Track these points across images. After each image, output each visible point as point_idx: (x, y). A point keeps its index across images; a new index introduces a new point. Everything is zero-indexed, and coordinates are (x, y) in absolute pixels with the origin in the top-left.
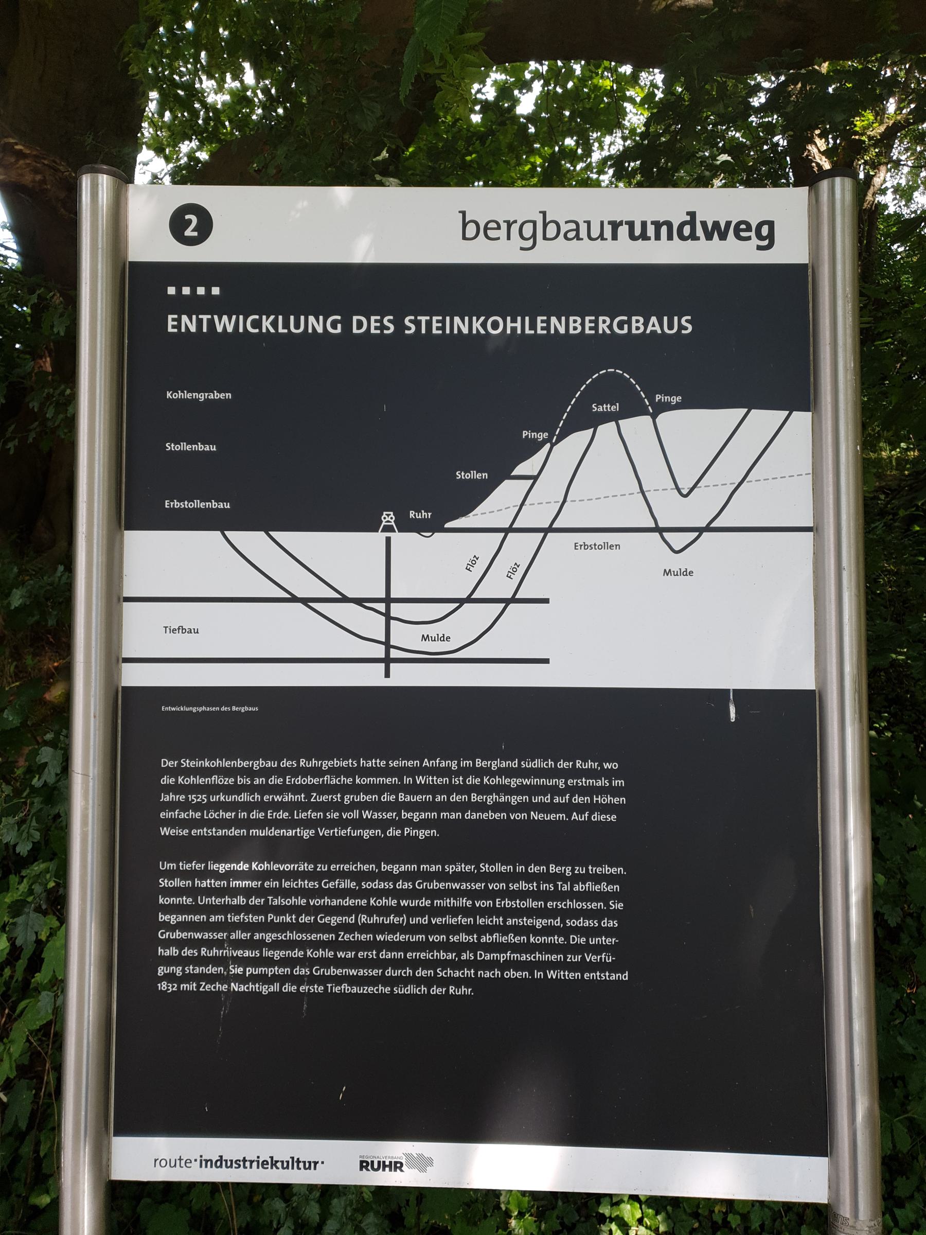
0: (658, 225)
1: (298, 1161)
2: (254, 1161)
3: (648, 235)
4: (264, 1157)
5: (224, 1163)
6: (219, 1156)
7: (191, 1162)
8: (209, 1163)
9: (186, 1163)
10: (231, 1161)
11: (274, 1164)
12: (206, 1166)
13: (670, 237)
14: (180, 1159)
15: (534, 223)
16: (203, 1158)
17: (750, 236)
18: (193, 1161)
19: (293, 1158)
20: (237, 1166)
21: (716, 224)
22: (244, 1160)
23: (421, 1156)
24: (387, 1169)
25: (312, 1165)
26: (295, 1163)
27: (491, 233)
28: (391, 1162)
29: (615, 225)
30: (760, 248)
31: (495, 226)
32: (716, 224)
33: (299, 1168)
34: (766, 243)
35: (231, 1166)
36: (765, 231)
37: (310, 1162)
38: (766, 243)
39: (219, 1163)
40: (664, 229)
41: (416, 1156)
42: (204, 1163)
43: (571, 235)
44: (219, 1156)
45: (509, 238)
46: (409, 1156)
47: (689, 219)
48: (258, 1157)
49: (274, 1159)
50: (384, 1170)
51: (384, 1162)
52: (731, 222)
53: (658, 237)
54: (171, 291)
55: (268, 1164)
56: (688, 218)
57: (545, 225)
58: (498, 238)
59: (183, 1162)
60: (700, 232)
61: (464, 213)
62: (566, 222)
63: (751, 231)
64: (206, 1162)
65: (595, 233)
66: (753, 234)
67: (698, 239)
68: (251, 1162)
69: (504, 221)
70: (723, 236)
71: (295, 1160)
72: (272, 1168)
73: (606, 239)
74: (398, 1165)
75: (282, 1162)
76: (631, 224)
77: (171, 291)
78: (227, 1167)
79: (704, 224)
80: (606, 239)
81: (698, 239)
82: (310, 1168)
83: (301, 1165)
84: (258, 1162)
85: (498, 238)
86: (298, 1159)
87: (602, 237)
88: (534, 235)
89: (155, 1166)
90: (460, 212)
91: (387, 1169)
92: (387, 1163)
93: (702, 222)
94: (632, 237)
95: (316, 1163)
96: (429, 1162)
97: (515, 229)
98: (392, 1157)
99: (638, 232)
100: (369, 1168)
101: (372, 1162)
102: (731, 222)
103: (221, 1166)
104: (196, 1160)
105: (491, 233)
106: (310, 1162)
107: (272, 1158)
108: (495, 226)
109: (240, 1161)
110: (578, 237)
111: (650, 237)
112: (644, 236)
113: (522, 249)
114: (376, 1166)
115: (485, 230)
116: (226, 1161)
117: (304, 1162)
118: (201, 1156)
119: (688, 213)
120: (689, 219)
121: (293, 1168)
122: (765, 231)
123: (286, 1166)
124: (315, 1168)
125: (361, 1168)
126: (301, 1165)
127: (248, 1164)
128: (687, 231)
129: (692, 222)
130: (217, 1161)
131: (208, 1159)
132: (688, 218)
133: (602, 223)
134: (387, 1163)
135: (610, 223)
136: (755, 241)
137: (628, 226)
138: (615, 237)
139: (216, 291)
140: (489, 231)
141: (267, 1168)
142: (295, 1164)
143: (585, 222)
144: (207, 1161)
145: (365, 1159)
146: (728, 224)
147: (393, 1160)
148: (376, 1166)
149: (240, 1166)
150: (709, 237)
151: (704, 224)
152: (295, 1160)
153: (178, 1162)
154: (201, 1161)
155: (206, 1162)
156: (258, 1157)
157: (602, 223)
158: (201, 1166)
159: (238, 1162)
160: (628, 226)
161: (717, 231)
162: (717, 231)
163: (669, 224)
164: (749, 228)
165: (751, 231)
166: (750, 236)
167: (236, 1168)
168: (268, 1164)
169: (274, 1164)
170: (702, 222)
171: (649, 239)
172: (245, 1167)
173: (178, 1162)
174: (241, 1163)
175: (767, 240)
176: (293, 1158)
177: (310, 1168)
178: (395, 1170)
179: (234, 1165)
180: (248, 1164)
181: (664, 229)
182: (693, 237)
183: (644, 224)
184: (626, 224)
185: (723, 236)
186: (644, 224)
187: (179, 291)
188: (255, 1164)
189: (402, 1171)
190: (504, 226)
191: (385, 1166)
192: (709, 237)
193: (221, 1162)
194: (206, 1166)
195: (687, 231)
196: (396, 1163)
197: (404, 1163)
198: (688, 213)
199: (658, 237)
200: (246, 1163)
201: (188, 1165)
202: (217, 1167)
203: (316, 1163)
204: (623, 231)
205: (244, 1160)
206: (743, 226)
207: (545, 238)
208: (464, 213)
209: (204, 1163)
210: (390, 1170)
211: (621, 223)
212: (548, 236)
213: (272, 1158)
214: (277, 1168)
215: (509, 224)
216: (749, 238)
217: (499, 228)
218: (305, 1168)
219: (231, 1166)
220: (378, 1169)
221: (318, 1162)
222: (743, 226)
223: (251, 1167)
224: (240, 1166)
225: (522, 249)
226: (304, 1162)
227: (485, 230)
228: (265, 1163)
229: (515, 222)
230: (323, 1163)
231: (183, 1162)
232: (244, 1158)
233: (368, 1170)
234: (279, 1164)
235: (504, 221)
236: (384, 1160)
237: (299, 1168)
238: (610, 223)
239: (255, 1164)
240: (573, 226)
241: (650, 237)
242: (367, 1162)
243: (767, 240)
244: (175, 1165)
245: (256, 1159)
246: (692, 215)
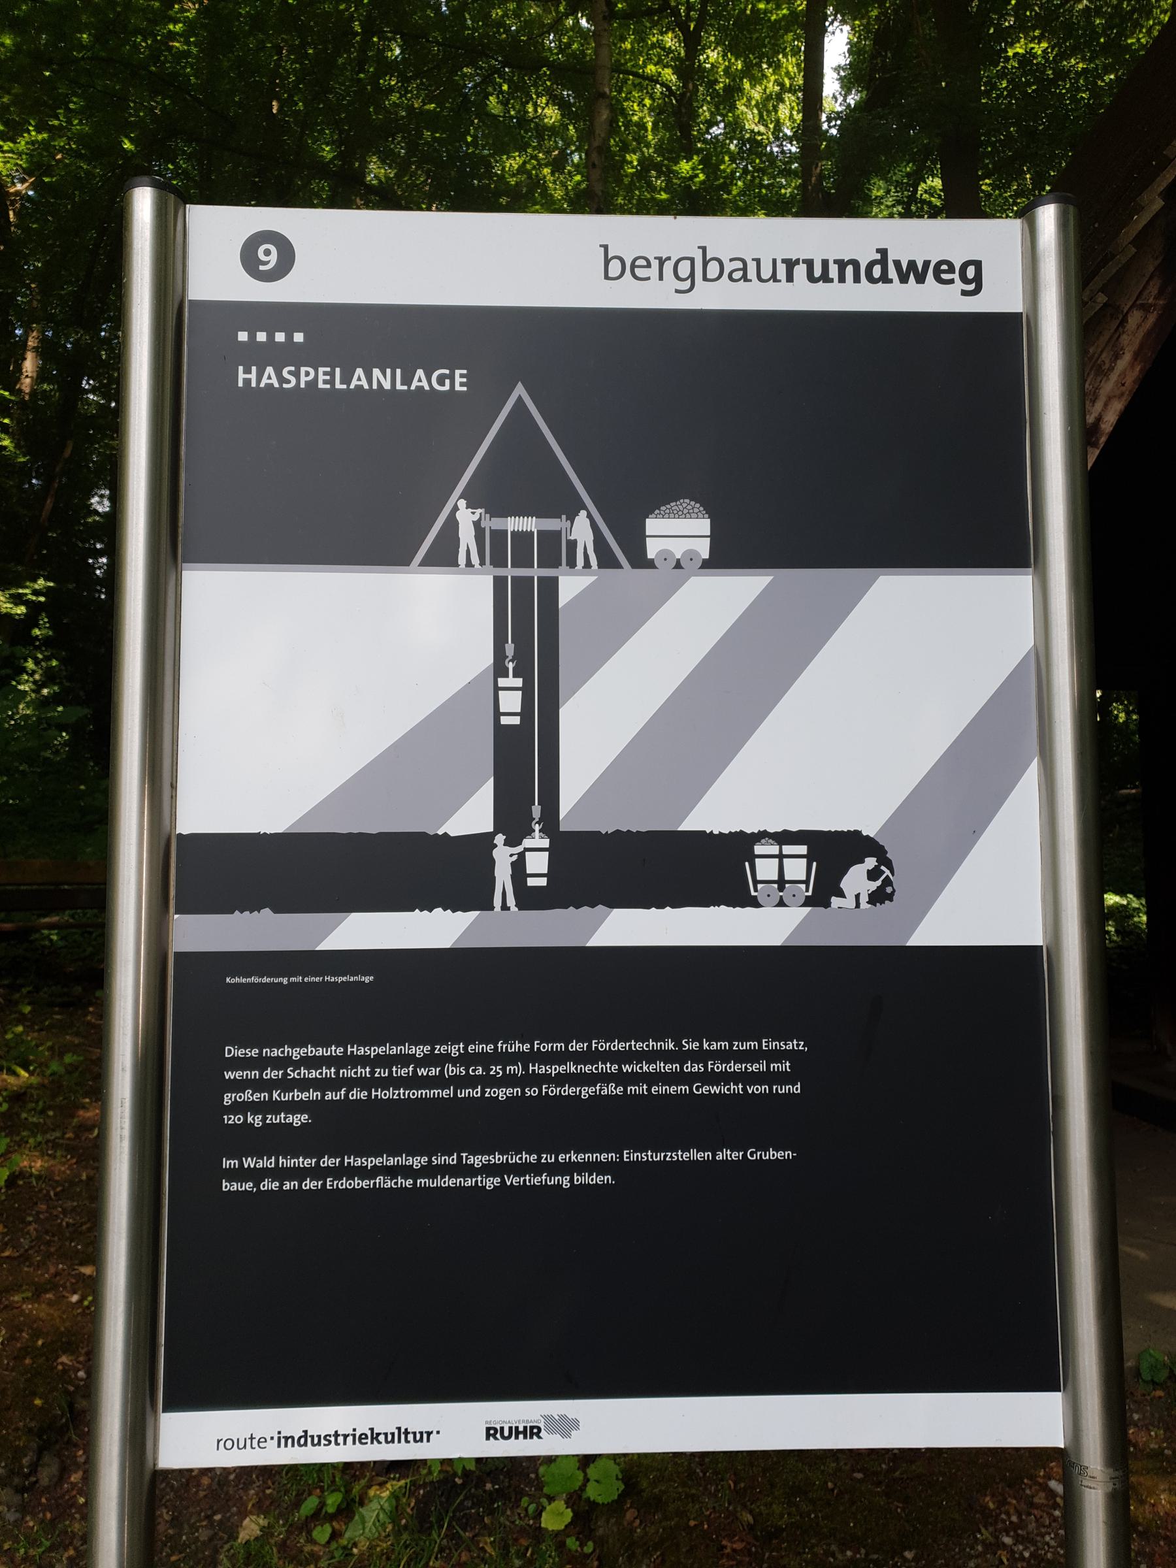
0: (842, 265)
1: (407, 1433)
2: (348, 1435)
3: (831, 276)
5: (309, 1440)
6: (303, 1431)
7: (266, 1441)
8: (290, 1441)
9: (259, 1442)
10: (319, 1437)
11: (375, 1437)
12: (286, 1445)
13: (857, 279)
14: (252, 1438)
15: (692, 260)
16: (282, 1435)
17: (953, 279)
18: (268, 1439)
19: (399, 1429)
20: (327, 1443)
21: (912, 264)
22: (336, 1435)
24: (521, 1436)
25: (425, 1436)
26: (403, 1434)
27: (639, 272)
28: (525, 1428)
29: (790, 264)
30: (965, 293)
31: (644, 263)
32: (912, 264)
33: (407, 1441)
34: (972, 287)
35: (319, 1443)
36: (971, 272)
37: (421, 1433)
38: (972, 287)
40: (849, 270)
41: (557, 1418)
42: (283, 1441)
43: (737, 275)
44: (303, 1431)
45: (661, 278)
46: (548, 1418)
47: (879, 258)
48: (354, 1430)
49: (375, 1431)
50: (517, 1438)
51: (517, 1428)
52: (930, 261)
53: (842, 279)
55: (367, 1437)
56: (878, 256)
57: (705, 264)
58: (648, 279)
59: (255, 1442)
60: (892, 273)
61: (606, 247)
62: (731, 260)
63: (954, 273)
64: (285, 1440)
65: (766, 273)
66: (956, 276)
67: (891, 281)
68: (346, 1436)
69: (655, 258)
70: (921, 279)
71: (403, 1430)
72: (372, 1443)
73: (780, 281)
74: (535, 1431)
75: (386, 1434)
76: (810, 263)
77: (243, 336)
78: (313, 1445)
79: (897, 264)
80: (780, 281)
81: (891, 281)
82: (421, 1440)
83: (410, 1437)
84: (354, 1436)
85: (648, 279)
86: (406, 1430)
87: (774, 278)
88: (692, 275)
89: (218, 1449)
90: (601, 246)
91: (521, 1436)
92: (521, 1429)
93: (894, 261)
94: (811, 278)
95: (429, 1434)
97: (668, 267)
98: (527, 1421)
99: (818, 272)
100: (498, 1436)
101: (502, 1429)
102: (929, 262)
103: (305, 1444)
104: (272, 1438)
105: (639, 272)
106: (421, 1433)
107: (372, 1430)
108: (644, 263)
109: (330, 1436)
110: (745, 278)
111: (833, 279)
112: (825, 278)
113: (677, 291)
114: (506, 1434)
115: (632, 268)
116: (312, 1437)
117: (414, 1433)
118: (279, 1433)
119: (878, 251)
120: (879, 258)
121: (399, 1441)
122: (971, 272)
123: (390, 1439)
124: (428, 1440)
125: (488, 1438)
126: (410, 1437)
127: (340, 1440)
128: (877, 271)
129: (883, 262)
130: (300, 1438)
131: (289, 1435)
132: (878, 256)
133: (774, 261)
134: (521, 1429)
135: (784, 261)
136: (959, 285)
137: (805, 265)
138: (790, 278)
139: (299, 337)
140: (636, 269)
141: (366, 1443)
142: (403, 1436)
143: (753, 260)
144: (286, 1438)
145: (493, 1426)
146: (927, 264)
147: (528, 1425)
148: (506, 1434)
149: (330, 1442)
150: (904, 279)
151: (897, 264)
152: (403, 1430)
153: (248, 1442)
154: (279, 1439)
155: (285, 1440)
156: (354, 1430)
157: (774, 261)
158: (279, 1446)
159: (328, 1438)
160: (805, 265)
161: (913, 272)
162: (913, 272)
163: (855, 264)
164: (951, 269)
165: (954, 273)
166: (953, 279)
167: (325, 1445)
168: (367, 1437)
169: (375, 1437)
170: (894, 261)
171: (831, 281)
172: (337, 1444)
173: (248, 1442)
174: (333, 1439)
175: (974, 285)
176: (399, 1429)
177: (421, 1440)
178: (531, 1437)
179: (323, 1442)
180: (340, 1440)
181: (849, 270)
182: (885, 278)
183: (825, 263)
184: (803, 263)
185: (921, 279)
186: (825, 263)
187: (252, 336)
188: (350, 1439)
189: (540, 1437)
190: (655, 264)
191: (518, 1433)
192: (904, 279)
193: (305, 1439)
194: (286, 1445)
195: (877, 271)
196: (532, 1428)
197: (542, 1428)
198: (878, 251)
199: (842, 279)
200: (339, 1438)
201: (261, 1445)
202: (300, 1445)
203: (429, 1434)
204: (800, 271)
205: (336, 1435)
206: (944, 267)
207: (705, 278)
208: (606, 247)
209: (283, 1441)
210: (525, 1437)
211: (797, 262)
212: (709, 277)
213: (372, 1430)
214: (379, 1442)
215: (662, 262)
216: (952, 281)
217: (649, 265)
218: (415, 1441)
219: (319, 1443)
221: (432, 1432)
222: (944, 267)
223: (345, 1443)
224: (330, 1442)
225: (677, 291)
226: (414, 1433)
227: (632, 268)
228: (363, 1436)
229: (669, 258)
230: (438, 1432)
231: (255, 1442)
232: (336, 1432)
233: (496, 1439)
234: (382, 1438)
235: (655, 258)
236: (517, 1425)
237: (407, 1441)
238: (784, 261)
239: (350, 1439)
240: (740, 265)
241: (833, 279)
242: (495, 1429)
243: (974, 284)
244: (245, 1447)
245: (352, 1432)
246: (883, 252)
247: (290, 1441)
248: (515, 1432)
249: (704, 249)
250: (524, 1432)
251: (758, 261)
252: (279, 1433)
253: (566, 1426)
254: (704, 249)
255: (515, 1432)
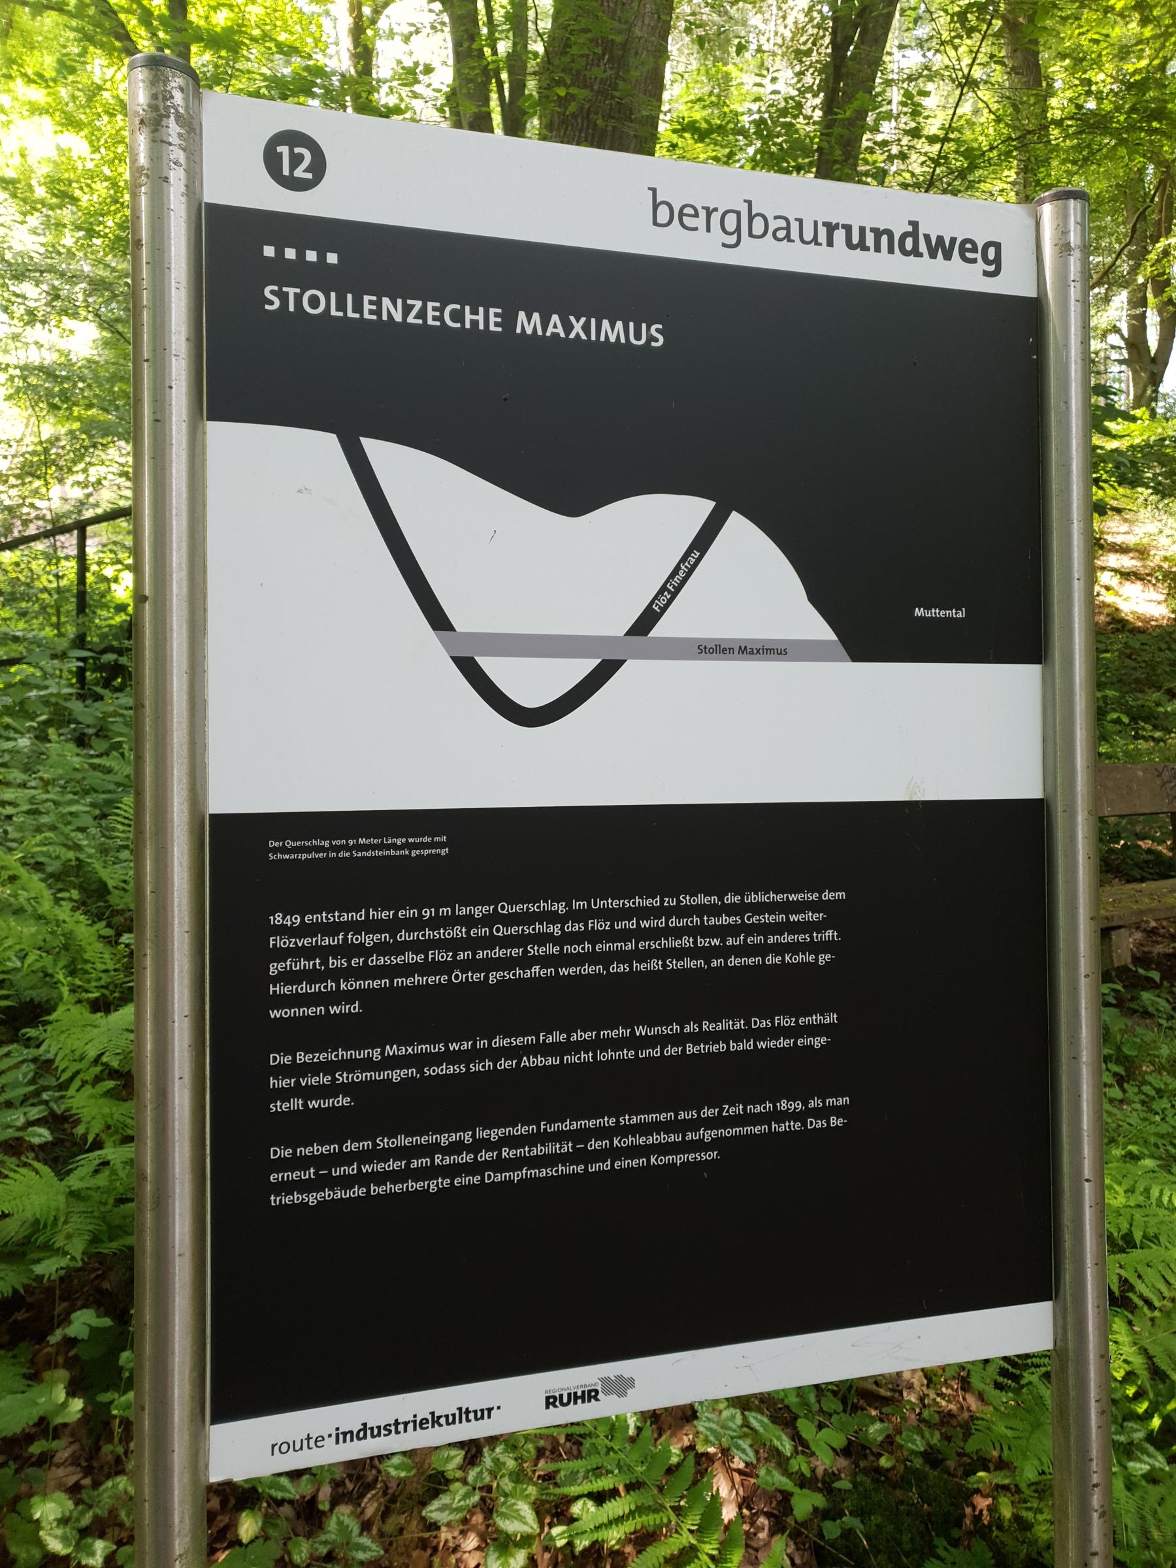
0: (878, 234)
1: (468, 1412)
4: (424, 1414)
5: (369, 1432)
9: (316, 1441)
12: (345, 1441)
14: (309, 1438)
15: (738, 214)
18: (326, 1437)
21: (940, 239)
23: (620, 1378)
24: (579, 1401)
25: (486, 1413)
27: (688, 221)
28: (583, 1392)
29: (831, 228)
30: (986, 274)
32: (940, 239)
33: (468, 1420)
34: (992, 268)
35: (379, 1434)
37: (482, 1411)
38: (992, 268)
39: (362, 1434)
40: (884, 239)
42: (341, 1437)
45: (708, 230)
50: (575, 1403)
51: (575, 1393)
54: (269, 251)
55: (427, 1422)
56: (910, 229)
59: (312, 1442)
60: (923, 248)
62: (776, 218)
64: (343, 1436)
65: (808, 236)
66: (978, 256)
68: (406, 1424)
69: (703, 208)
70: (948, 256)
75: (447, 1416)
76: (848, 229)
81: (921, 255)
83: (471, 1416)
84: (415, 1422)
91: (579, 1401)
92: (579, 1394)
94: (850, 245)
95: (490, 1410)
96: (630, 1383)
97: (715, 218)
99: (855, 240)
100: (557, 1403)
101: (561, 1396)
104: (330, 1436)
105: (688, 221)
110: (788, 237)
112: (862, 245)
113: (724, 245)
114: (565, 1400)
116: (372, 1429)
117: (475, 1412)
119: (911, 223)
123: (451, 1420)
124: (489, 1417)
125: (547, 1407)
126: (471, 1416)
127: (401, 1428)
129: (914, 234)
132: (910, 229)
133: (816, 223)
134: (579, 1394)
136: (981, 266)
138: (830, 243)
140: (684, 218)
142: (464, 1416)
144: (345, 1434)
146: (953, 240)
148: (565, 1400)
149: (390, 1431)
150: (933, 255)
153: (305, 1442)
154: (337, 1435)
156: (415, 1416)
157: (816, 223)
158: (337, 1442)
168: (427, 1422)
169: (436, 1420)
171: (868, 249)
172: (397, 1432)
173: (305, 1442)
174: (393, 1428)
176: (460, 1409)
177: (482, 1417)
178: (589, 1401)
179: (383, 1432)
180: (401, 1428)
182: (916, 252)
185: (948, 256)
188: (410, 1426)
189: (597, 1400)
191: (576, 1398)
194: (345, 1441)
196: (590, 1391)
198: (911, 223)
203: (490, 1410)
204: (840, 235)
205: (397, 1423)
206: (968, 246)
207: (751, 235)
209: (341, 1437)
210: (583, 1402)
211: (837, 226)
213: (433, 1414)
214: (440, 1425)
215: (709, 212)
216: (974, 261)
217: (696, 215)
218: (476, 1419)
219: (379, 1434)
220: (568, 1403)
222: (968, 246)
223: (405, 1431)
224: (390, 1431)
225: (724, 245)
226: (475, 1412)
229: (716, 210)
232: (396, 1420)
233: (556, 1406)
234: (443, 1421)
235: (703, 208)
237: (468, 1420)
238: (824, 224)
239: (410, 1426)
242: (555, 1398)
244: (301, 1448)
246: (915, 224)
247: (348, 1436)
248: (574, 1398)
249: (749, 203)
250: (583, 1398)
251: (800, 221)
252: (337, 1429)
253: (621, 1386)
254: (749, 203)
255: (574, 1398)
